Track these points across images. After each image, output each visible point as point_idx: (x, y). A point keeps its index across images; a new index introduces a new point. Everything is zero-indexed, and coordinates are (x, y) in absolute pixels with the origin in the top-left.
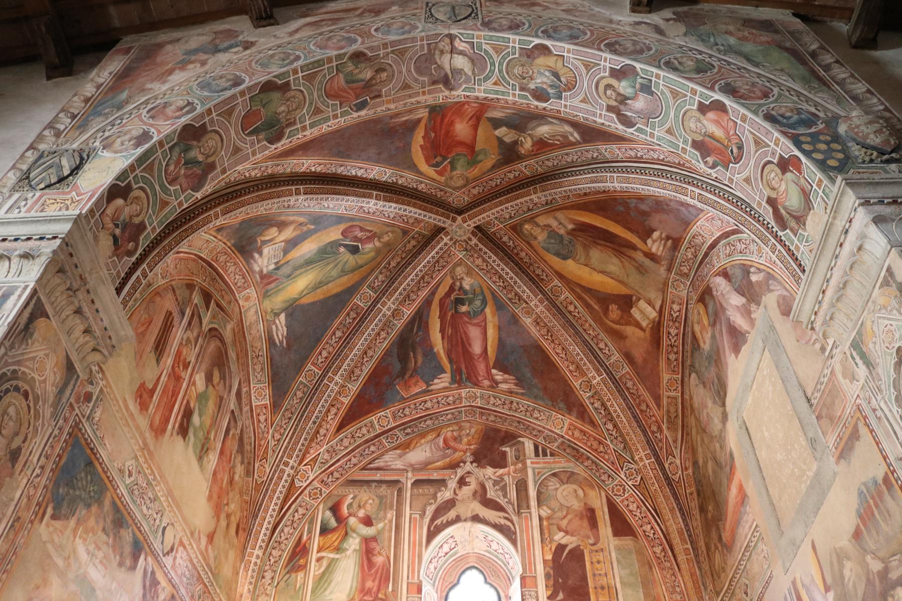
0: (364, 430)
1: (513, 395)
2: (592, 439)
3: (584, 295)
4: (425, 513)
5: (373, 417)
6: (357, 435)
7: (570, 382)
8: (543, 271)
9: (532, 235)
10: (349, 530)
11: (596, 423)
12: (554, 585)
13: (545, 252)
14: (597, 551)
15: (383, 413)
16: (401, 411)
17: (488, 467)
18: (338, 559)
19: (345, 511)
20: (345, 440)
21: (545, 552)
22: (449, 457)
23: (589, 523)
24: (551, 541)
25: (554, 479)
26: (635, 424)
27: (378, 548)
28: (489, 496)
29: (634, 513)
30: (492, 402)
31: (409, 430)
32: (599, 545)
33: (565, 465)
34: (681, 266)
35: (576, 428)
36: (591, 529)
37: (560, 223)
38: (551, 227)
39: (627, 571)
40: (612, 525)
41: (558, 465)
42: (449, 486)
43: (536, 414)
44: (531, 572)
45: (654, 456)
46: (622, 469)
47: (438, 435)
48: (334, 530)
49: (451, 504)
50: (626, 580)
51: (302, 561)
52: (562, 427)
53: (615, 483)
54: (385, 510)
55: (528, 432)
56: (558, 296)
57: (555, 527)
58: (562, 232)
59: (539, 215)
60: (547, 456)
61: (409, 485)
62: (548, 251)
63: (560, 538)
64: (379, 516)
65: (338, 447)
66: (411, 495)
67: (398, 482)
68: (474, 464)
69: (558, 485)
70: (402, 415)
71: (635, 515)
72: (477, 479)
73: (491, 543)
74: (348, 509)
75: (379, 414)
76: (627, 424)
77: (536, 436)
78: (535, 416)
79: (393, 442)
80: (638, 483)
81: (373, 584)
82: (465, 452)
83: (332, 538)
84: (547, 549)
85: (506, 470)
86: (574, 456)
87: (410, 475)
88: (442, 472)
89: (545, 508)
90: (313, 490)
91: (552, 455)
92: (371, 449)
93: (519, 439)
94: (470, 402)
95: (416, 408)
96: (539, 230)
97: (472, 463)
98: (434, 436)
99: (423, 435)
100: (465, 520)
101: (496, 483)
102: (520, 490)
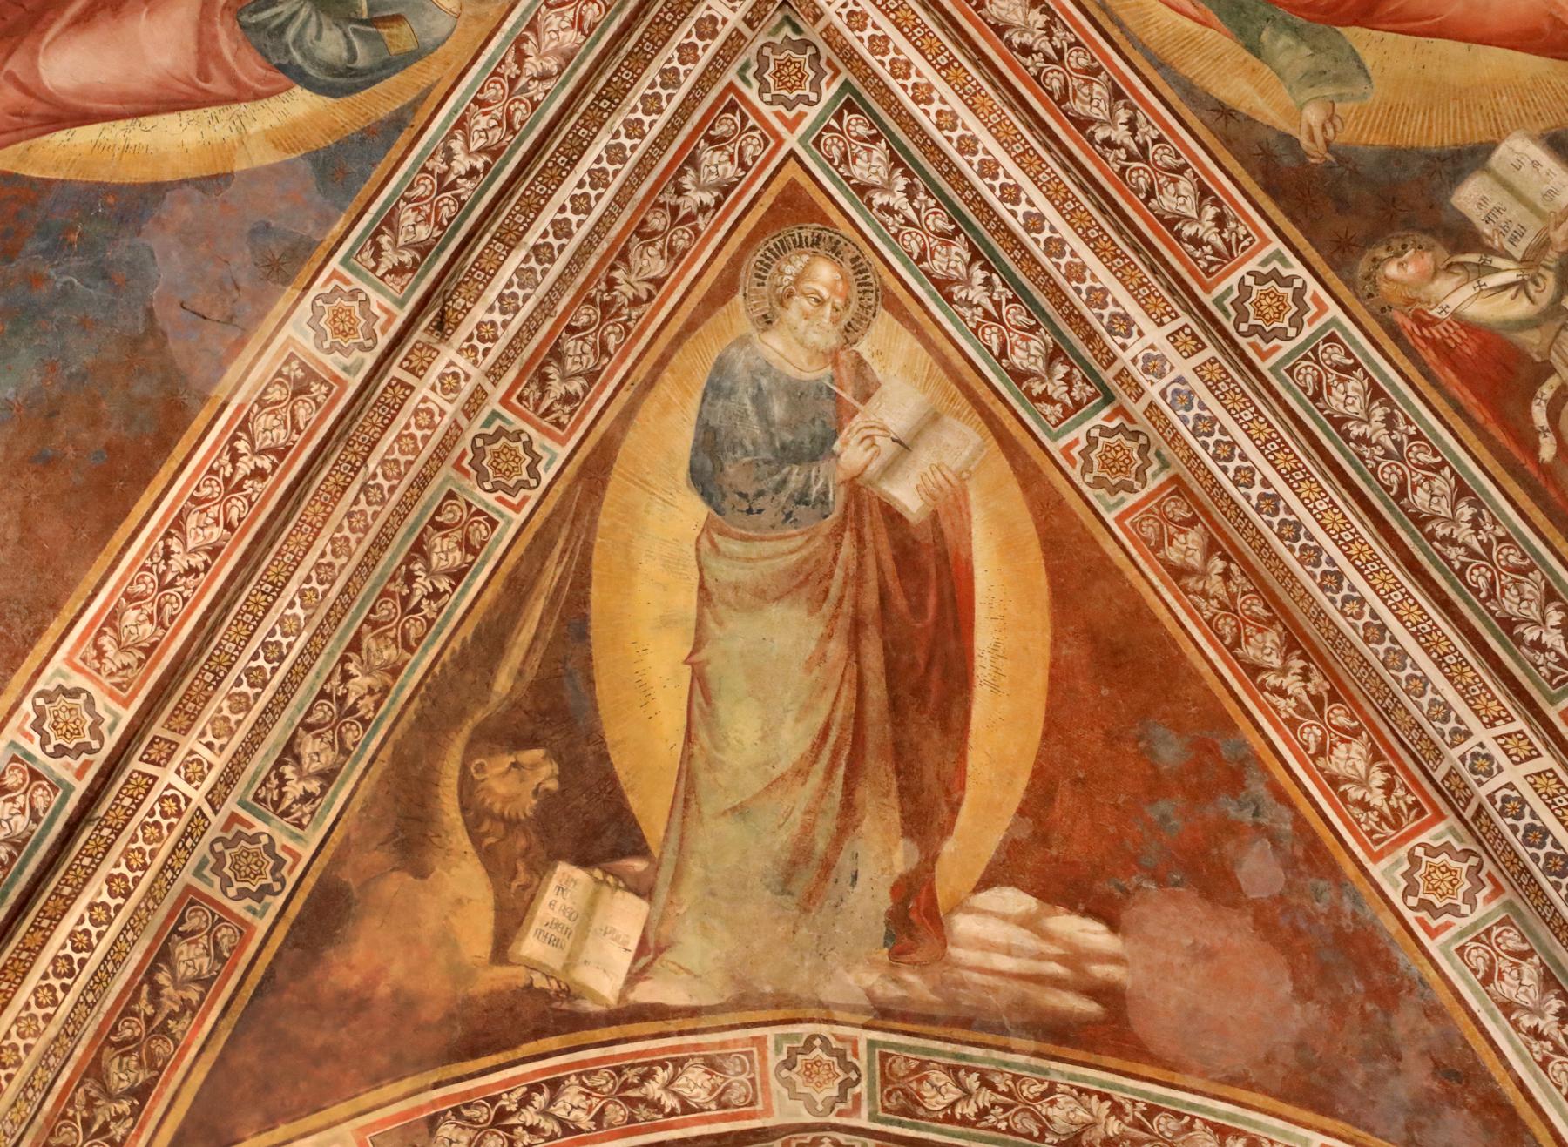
3: (537, 608)
7: (56, 627)
8: (592, 376)
9: (783, 300)
13: (701, 379)
34: (952, 1071)
37: (904, 446)
38: (866, 397)
56: (482, 477)
58: (852, 454)
59: (920, 333)
62: (716, 389)
96: (824, 334)
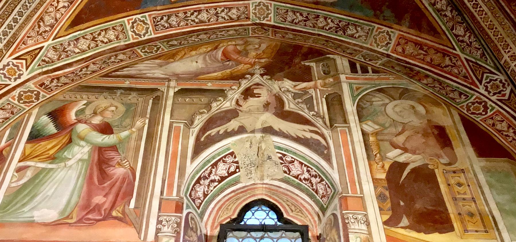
0: (111, 35)
1: (319, 7)
2: (434, 52)
4: (192, 122)
5: (125, 19)
6: (101, 38)
10: (74, 138)
11: (439, 30)
14: (454, 172)
15: (139, 16)
16: (165, 18)
17: (285, 79)
18: (52, 169)
19: (72, 116)
20: (82, 41)
24: (383, 158)
25: (380, 95)
26: (499, 14)
27: (117, 159)
28: (287, 108)
30: (289, 19)
31: (175, 43)
32: (456, 165)
33: (396, 81)
35: (407, 41)
36: (442, 148)
39: (507, 197)
40: (474, 144)
41: (384, 81)
43: (351, 31)
44: (354, 190)
46: (480, 82)
47: (216, 48)
48: (51, 137)
49: (233, 114)
50: (507, 208)
52: (388, 44)
53: (471, 100)
54: (134, 117)
55: (339, 49)
57: (387, 144)
60: (368, 72)
61: (171, 93)
63: (394, 154)
64: (124, 124)
65: (71, 48)
68: (265, 77)
69: (387, 101)
70: (166, 25)
72: (270, 91)
73: (291, 166)
74: (76, 115)
75: (134, 17)
76: (489, 14)
77: (351, 54)
78: (349, 32)
79: (152, 52)
80: (506, 97)
82: (253, 65)
83: (48, 144)
85: (311, 84)
86: (406, 74)
87: (173, 83)
88: (218, 82)
89: (370, 123)
90: (25, 92)
91: (374, 71)
92: (119, 58)
93: (328, 56)
94: (259, 18)
95: (186, 18)
97: (262, 75)
98: (209, 49)
99: (194, 47)
100: (253, 132)
101: (295, 96)
102: (332, 104)
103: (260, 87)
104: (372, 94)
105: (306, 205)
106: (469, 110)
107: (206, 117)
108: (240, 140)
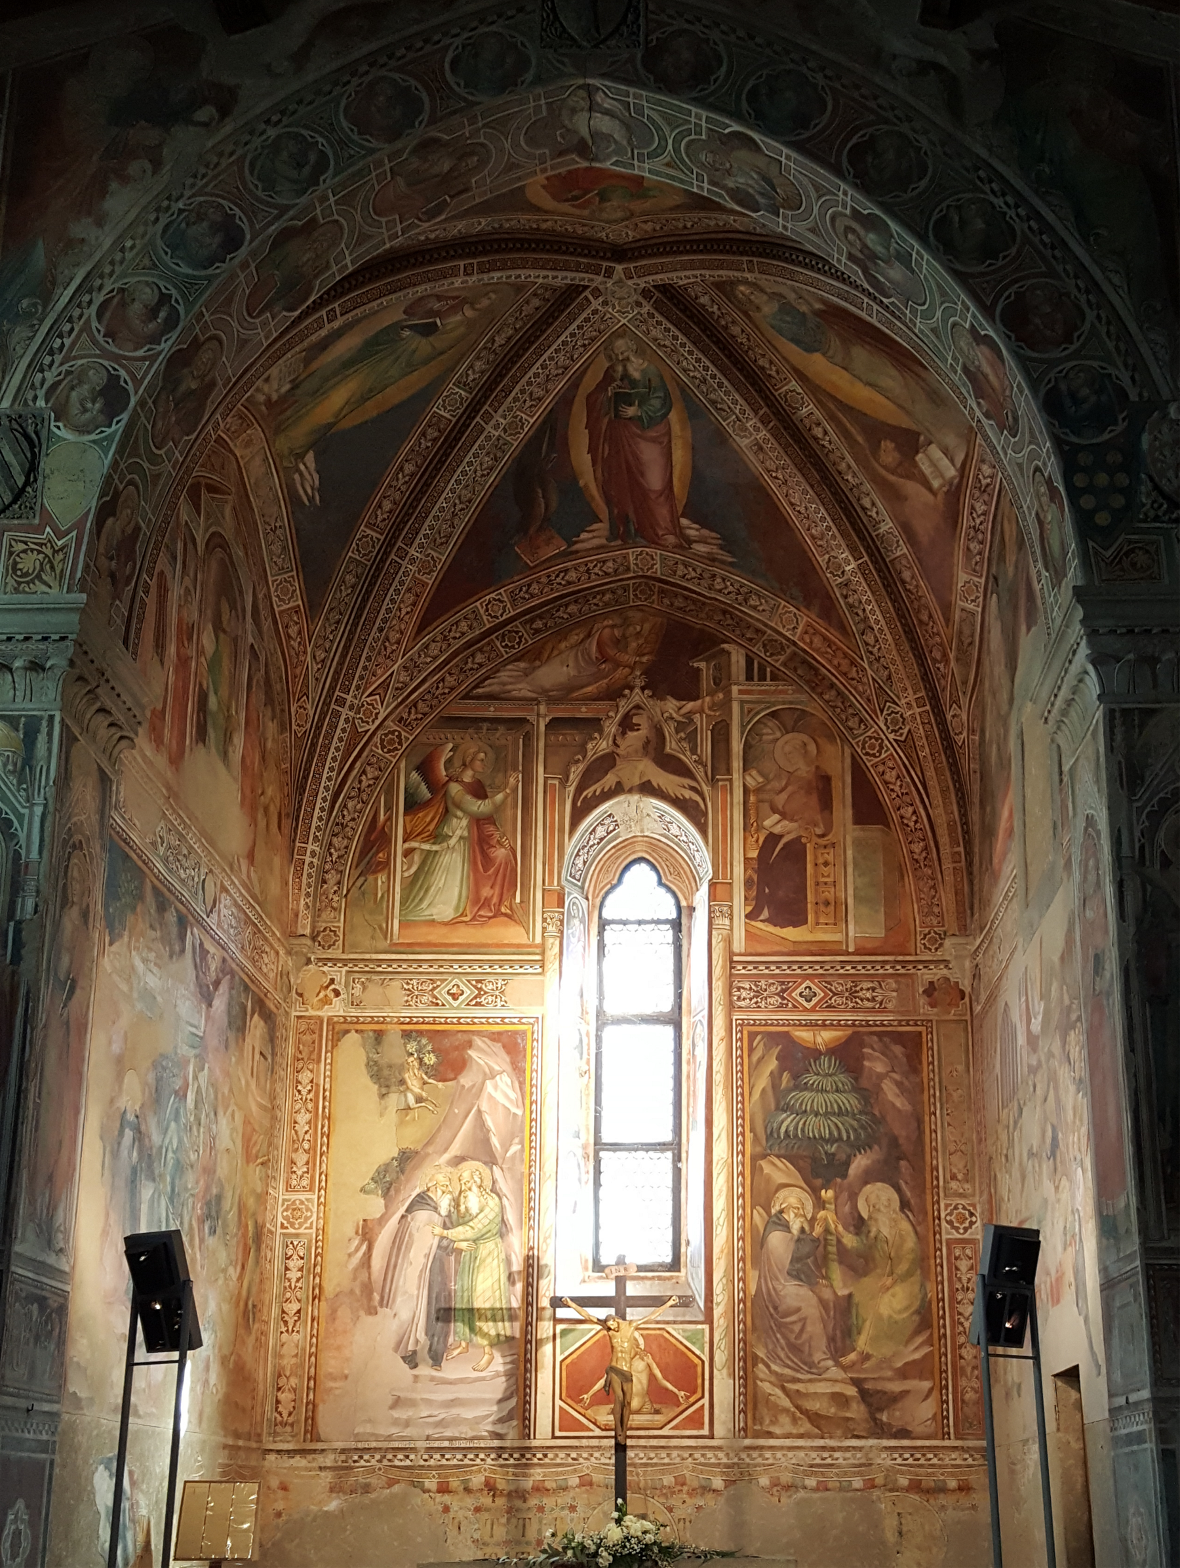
12: (757, 898)
18: (436, 852)
21: (748, 846)
22: (605, 678)
23: (820, 800)
24: (760, 828)
25: (772, 723)
27: (497, 835)
29: (891, 787)
40: (854, 805)
41: (781, 698)
42: (606, 730)
44: (724, 874)
45: (930, 699)
46: (882, 711)
48: (427, 804)
49: (608, 762)
51: (381, 855)
53: (869, 734)
61: (542, 728)
63: (771, 822)
64: (497, 781)
66: (546, 746)
67: (524, 721)
69: (778, 734)
71: (892, 790)
72: (650, 719)
74: (446, 769)
80: (902, 739)
81: (491, 892)
82: (633, 669)
84: (752, 840)
85: (700, 702)
86: (808, 682)
87: (543, 709)
89: (754, 773)
97: (643, 689)
100: (630, 791)
101: (680, 727)
103: (641, 711)
104: (765, 720)
105: (685, 866)
106: (863, 748)
107: (581, 767)
108: (618, 803)
